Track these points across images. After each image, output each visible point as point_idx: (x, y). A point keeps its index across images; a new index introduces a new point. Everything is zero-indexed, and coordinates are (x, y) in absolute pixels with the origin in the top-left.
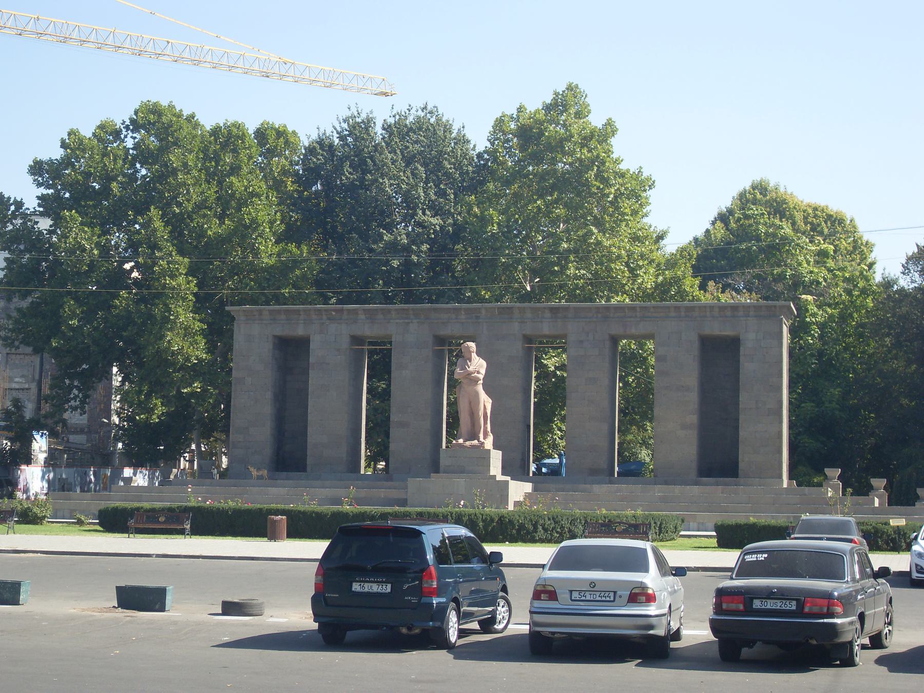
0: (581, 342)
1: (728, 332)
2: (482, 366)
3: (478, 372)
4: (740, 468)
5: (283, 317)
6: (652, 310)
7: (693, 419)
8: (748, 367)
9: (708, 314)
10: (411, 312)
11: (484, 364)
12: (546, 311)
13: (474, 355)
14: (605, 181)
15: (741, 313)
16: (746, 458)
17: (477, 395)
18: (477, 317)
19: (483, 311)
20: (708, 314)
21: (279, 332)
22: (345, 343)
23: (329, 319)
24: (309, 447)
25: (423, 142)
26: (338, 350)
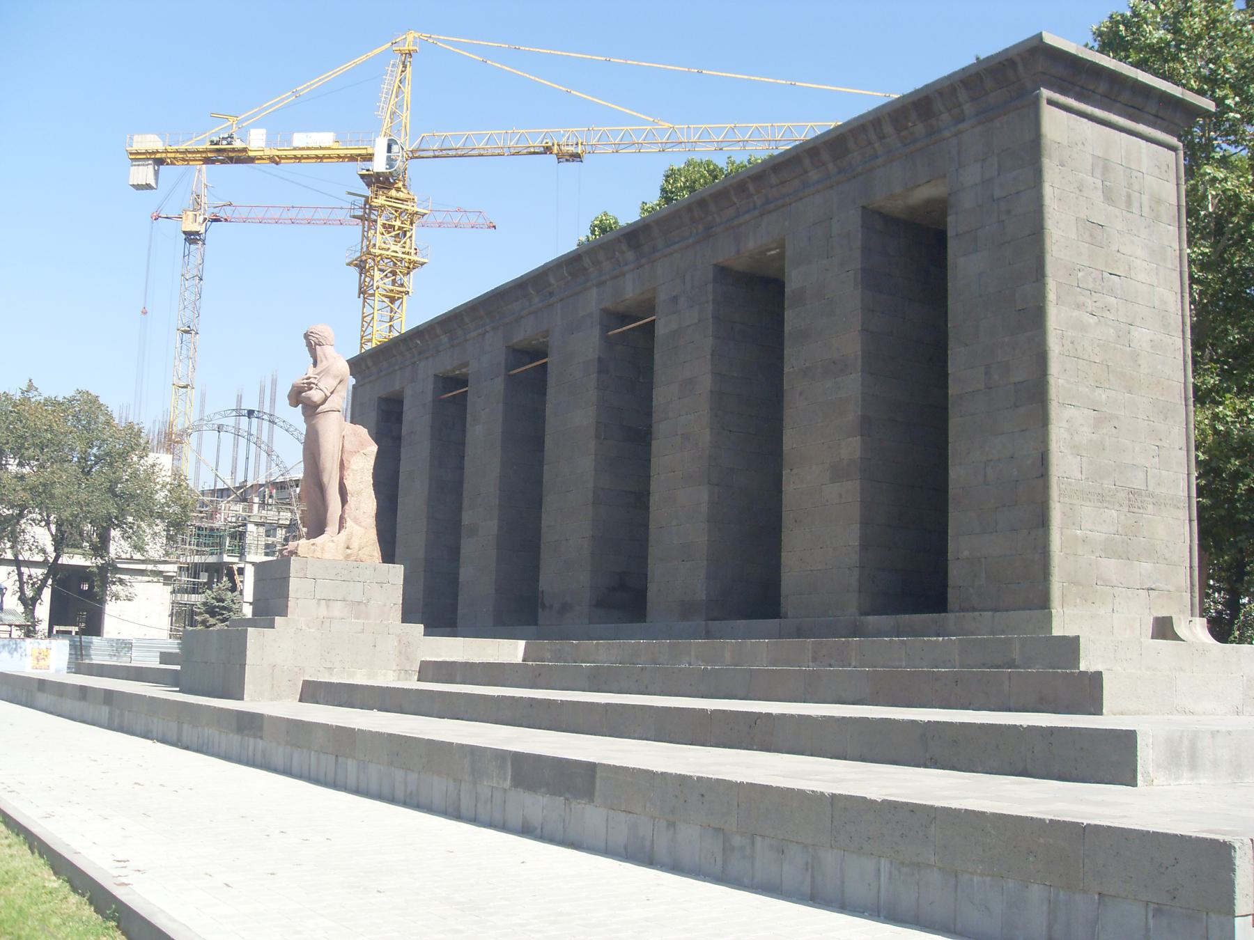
0: (675, 299)
4: (950, 583)
6: (774, 180)
8: (967, 268)
16: (966, 546)
18: (551, 294)
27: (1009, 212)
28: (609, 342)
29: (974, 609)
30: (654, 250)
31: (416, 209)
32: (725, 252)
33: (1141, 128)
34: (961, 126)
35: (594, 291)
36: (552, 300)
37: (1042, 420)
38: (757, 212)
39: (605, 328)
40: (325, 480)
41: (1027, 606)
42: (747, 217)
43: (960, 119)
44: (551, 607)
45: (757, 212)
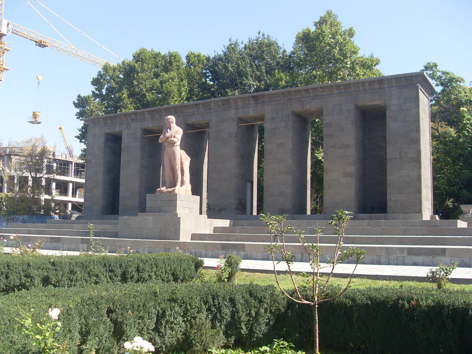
0: (274, 118)
1: (377, 102)
2: (177, 132)
3: (174, 137)
4: (388, 206)
5: (110, 122)
6: (320, 90)
7: (352, 169)
8: (393, 126)
9: (361, 88)
10: (172, 110)
11: (181, 131)
12: (251, 99)
13: (174, 125)
14: (345, 56)
15: (386, 85)
16: (393, 197)
17: (174, 154)
18: (210, 109)
19: (212, 104)
20: (361, 88)
21: (108, 131)
22: (139, 133)
23: (131, 120)
24: (120, 199)
25: (260, 51)
26: (136, 138)
27: (407, 114)
28: (238, 127)
29: (396, 213)
30: (263, 102)
31: (6, 48)
32: (297, 108)
33: (425, 93)
34: (392, 89)
35: (233, 110)
36: (211, 111)
37: (420, 168)
38: (312, 98)
39: (238, 124)
40: (177, 168)
41: (414, 212)
42: (307, 99)
43: (391, 87)
44: (214, 209)
45: (312, 98)
